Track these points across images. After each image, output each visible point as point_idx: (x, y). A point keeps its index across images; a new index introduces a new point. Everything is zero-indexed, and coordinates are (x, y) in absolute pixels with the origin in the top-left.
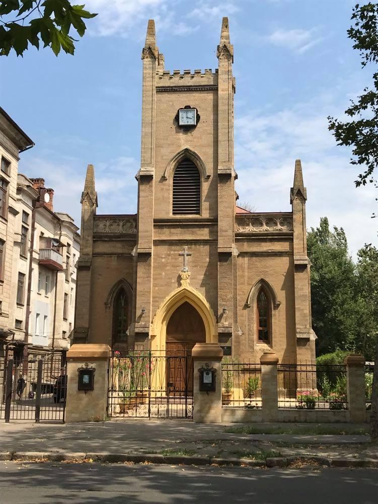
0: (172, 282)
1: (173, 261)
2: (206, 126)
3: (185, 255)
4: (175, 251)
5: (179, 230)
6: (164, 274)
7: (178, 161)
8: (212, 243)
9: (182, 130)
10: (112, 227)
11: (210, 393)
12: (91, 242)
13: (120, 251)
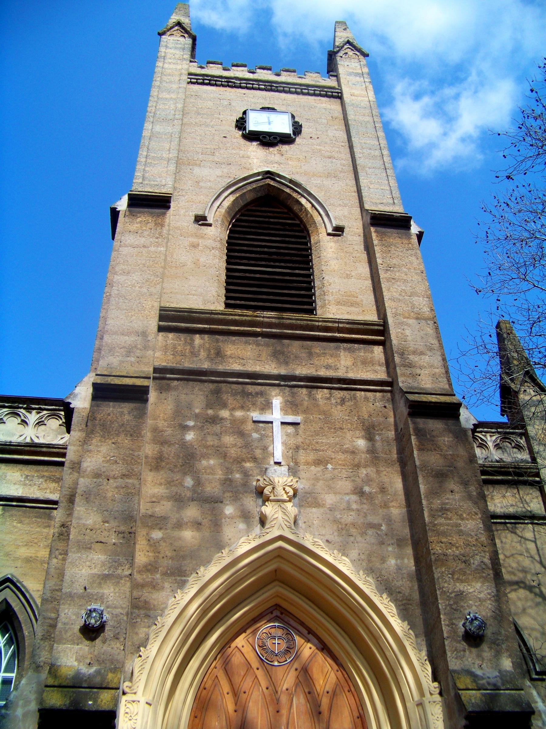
7: (244, 194)
8: (369, 394)
9: (255, 143)
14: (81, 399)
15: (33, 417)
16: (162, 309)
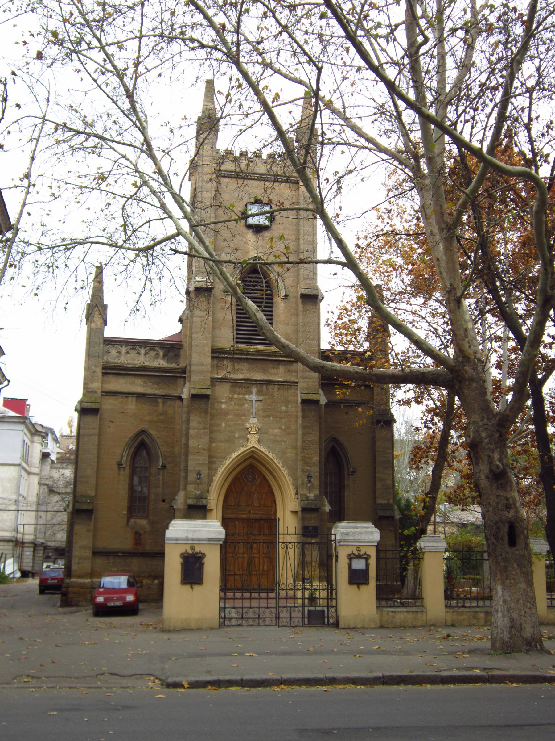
0: (235, 437)
1: (237, 407)
2: (283, 229)
3: (254, 401)
4: (239, 394)
5: (244, 366)
6: (223, 425)
9: (251, 231)
10: (128, 355)
11: (363, 588)
12: (100, 374)
13: (140, 390)
14: (185, 395)
15: (143, 351)
16: (212, 349)
